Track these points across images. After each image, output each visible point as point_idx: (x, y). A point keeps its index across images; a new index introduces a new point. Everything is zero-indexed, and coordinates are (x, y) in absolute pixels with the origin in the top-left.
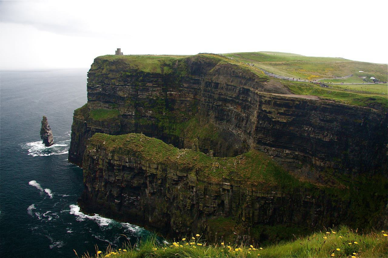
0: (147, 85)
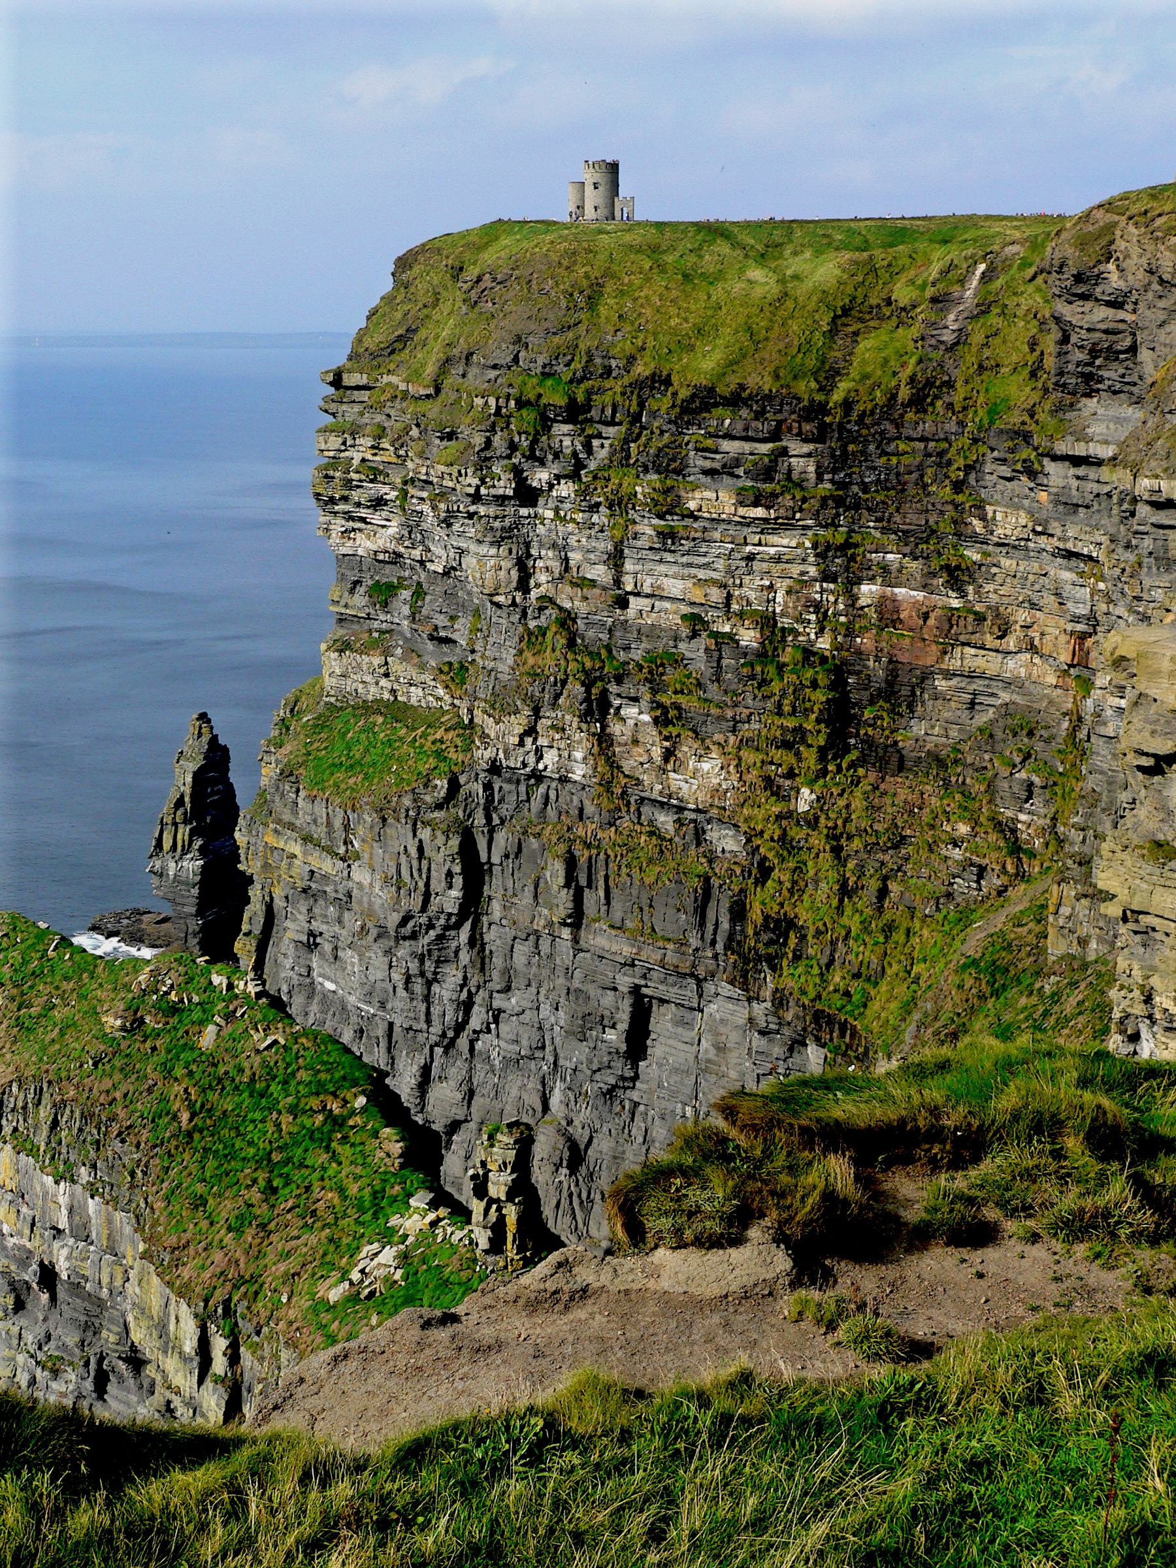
0: (692, 505)
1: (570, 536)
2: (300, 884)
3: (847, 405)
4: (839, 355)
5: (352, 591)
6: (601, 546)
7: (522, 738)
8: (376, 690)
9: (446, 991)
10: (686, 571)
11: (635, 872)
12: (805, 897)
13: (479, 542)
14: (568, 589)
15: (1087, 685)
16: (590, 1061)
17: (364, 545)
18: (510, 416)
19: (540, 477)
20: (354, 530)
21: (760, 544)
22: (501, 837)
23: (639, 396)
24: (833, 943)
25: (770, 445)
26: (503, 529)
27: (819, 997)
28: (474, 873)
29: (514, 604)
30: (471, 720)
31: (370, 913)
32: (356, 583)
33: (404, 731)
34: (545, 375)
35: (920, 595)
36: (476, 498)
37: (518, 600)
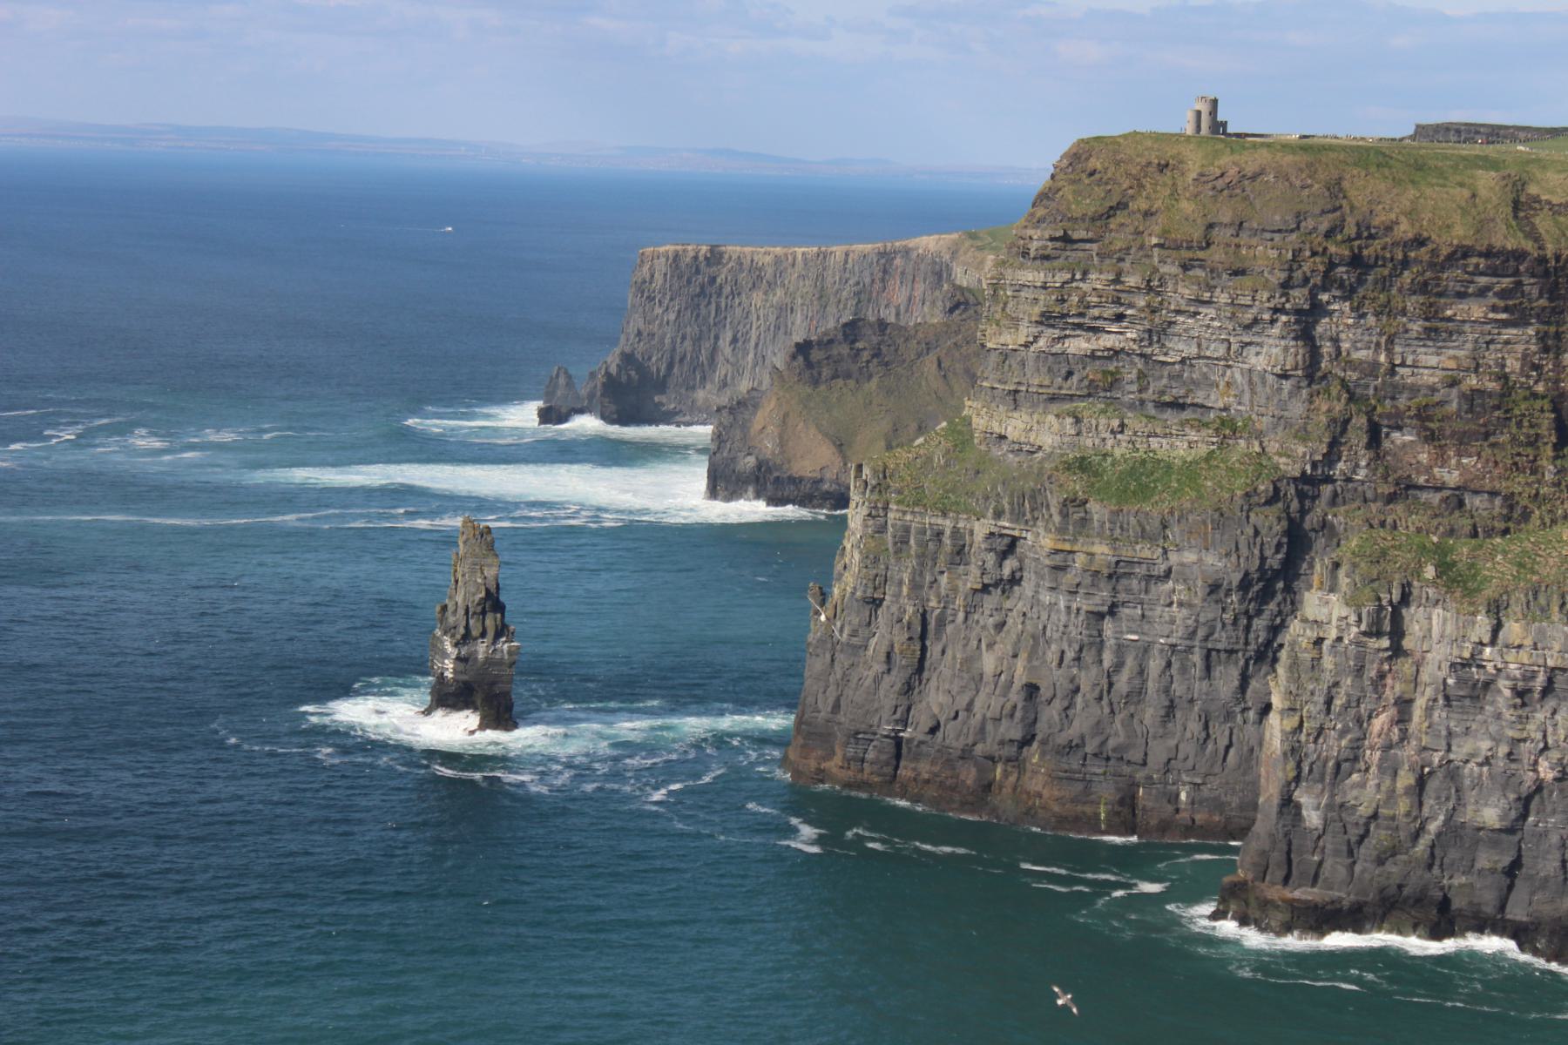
0: (1449, 313)
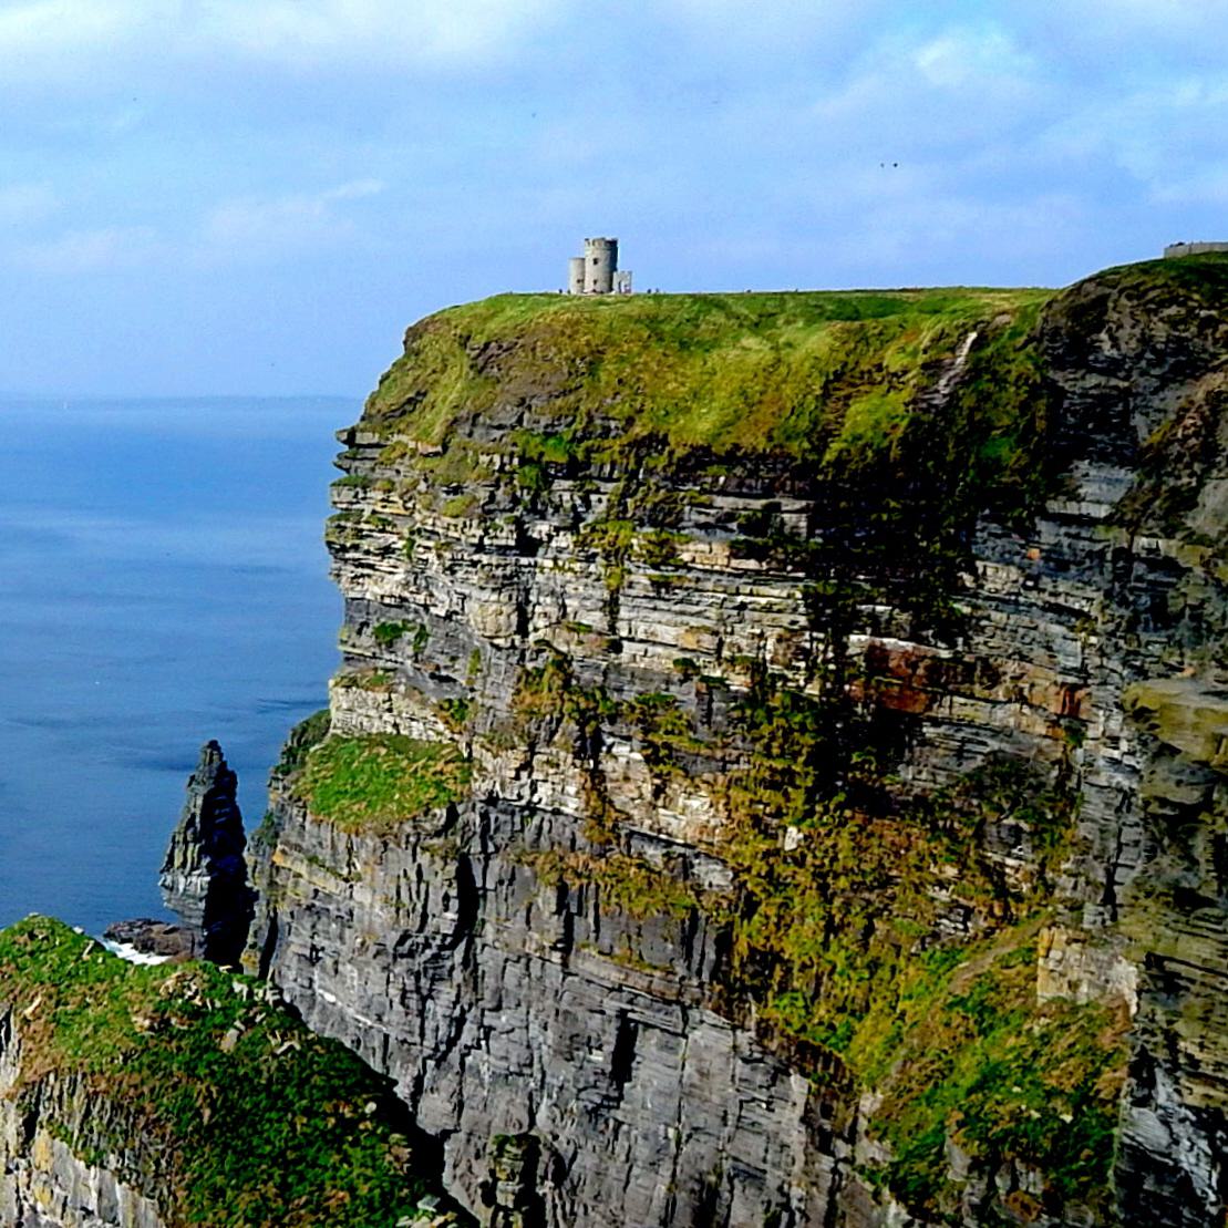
0: (686, 557)
1: (568, 585)
2: (305, 903)
3: (840, 463)
4: (831, 417)
5: (359, 632)
6: (597, 594)
7: (518, 770)
8: (381, 724)
9: (439, 1008)
10: (679, 619)
11: (624, 901)
12: (791, 931)
13: (482, 588)
14: (565, 633)
15: (1077, 735)
16: (576, 1080)
17: (372, 590)
18: (514, 472)
19: (540, 529)
20: (363, 576)
21: (751, 594)
22: (495, 864)
23: (637, 455)
24: (818, 978)
25: (764, 502)
26: (504, 577)
27: (803, 1029)
28: (470, 897)
29: (513, 646)
30: (470, 754)
31: (370, 931)
32: (365, 624)
33: (404, 763)
34: (548, 435)
35: (909, 646)
36: (480, 548)
37: (517, 643)
